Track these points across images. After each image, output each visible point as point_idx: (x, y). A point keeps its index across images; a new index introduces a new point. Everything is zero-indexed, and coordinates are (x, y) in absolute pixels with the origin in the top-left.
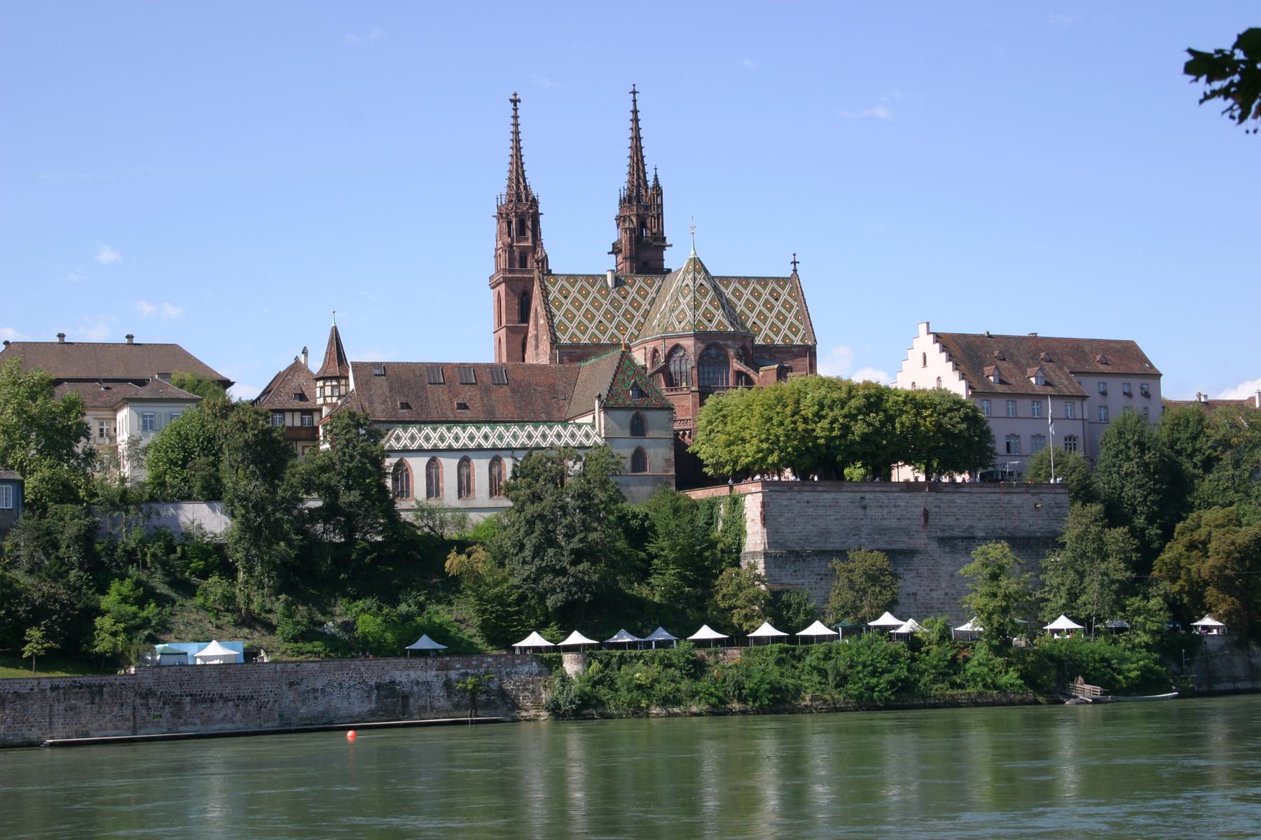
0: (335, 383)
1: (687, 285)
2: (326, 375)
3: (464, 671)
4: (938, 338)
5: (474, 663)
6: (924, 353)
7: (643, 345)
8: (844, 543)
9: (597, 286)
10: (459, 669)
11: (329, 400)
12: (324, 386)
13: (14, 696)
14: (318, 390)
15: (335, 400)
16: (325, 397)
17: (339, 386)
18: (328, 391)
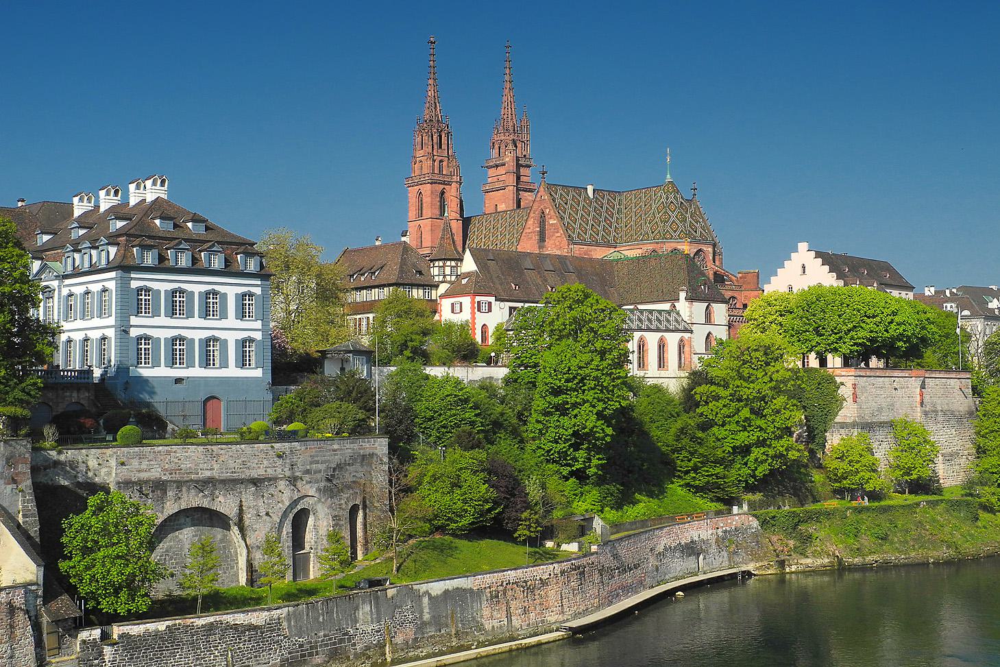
0: (453, 263)
1: (672, 202)
2: (448, 257)
3: (724, 529)
4: (818, 255)
5: (729, 521)
6: (804, 267)
7: (641, 246)
8: (888, 416)
9: (583, 197)
10: (722, 527)
11: (448, 278)
12: (443, 267)
13: (540, 582)
14: (436, 270)
15: (453, 278)
16: (445, 276)
17: (457, 266)
18: (448, 271)
